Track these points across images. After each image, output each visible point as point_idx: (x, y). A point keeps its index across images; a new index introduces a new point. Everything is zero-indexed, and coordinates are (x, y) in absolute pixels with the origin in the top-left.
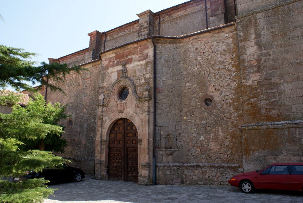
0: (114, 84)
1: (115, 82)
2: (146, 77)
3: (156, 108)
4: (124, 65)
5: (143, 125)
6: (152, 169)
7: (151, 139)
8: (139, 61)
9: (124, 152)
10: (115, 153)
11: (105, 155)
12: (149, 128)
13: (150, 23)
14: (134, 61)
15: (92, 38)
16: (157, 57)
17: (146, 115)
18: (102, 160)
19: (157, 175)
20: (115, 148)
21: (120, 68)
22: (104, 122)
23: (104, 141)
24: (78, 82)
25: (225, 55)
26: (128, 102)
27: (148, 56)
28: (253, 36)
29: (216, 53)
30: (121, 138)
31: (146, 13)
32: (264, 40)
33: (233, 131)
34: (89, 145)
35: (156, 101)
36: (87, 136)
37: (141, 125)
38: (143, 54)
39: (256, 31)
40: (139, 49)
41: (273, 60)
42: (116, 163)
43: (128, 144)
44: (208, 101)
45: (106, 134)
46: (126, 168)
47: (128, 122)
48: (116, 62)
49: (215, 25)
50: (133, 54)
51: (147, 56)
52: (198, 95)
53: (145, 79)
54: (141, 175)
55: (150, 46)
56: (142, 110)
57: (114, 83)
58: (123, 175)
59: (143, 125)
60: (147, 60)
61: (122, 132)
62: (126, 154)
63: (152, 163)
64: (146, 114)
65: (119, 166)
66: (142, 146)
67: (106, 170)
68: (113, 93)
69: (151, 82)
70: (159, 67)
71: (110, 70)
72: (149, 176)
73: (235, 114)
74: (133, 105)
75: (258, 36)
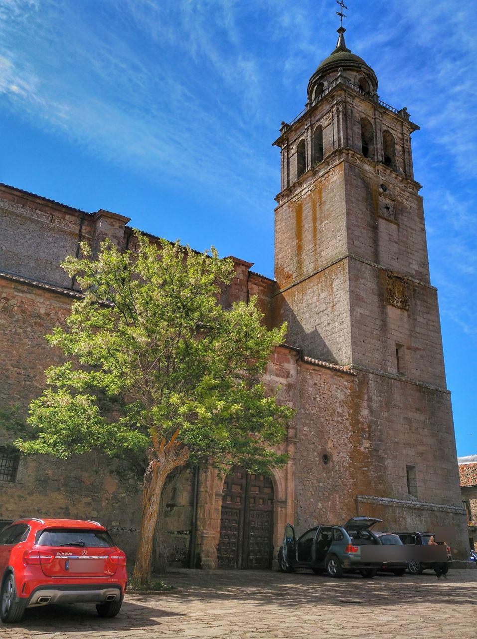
25: (344, 407)
28: (366, 397)
29: (336, 400)
31: (119, 220)
33: (349, 502)
41: (380, 431)
44: (326, 458)
52: (316, 447)
55: (292, 361)
65: (234, 543)
73: (351, 482)
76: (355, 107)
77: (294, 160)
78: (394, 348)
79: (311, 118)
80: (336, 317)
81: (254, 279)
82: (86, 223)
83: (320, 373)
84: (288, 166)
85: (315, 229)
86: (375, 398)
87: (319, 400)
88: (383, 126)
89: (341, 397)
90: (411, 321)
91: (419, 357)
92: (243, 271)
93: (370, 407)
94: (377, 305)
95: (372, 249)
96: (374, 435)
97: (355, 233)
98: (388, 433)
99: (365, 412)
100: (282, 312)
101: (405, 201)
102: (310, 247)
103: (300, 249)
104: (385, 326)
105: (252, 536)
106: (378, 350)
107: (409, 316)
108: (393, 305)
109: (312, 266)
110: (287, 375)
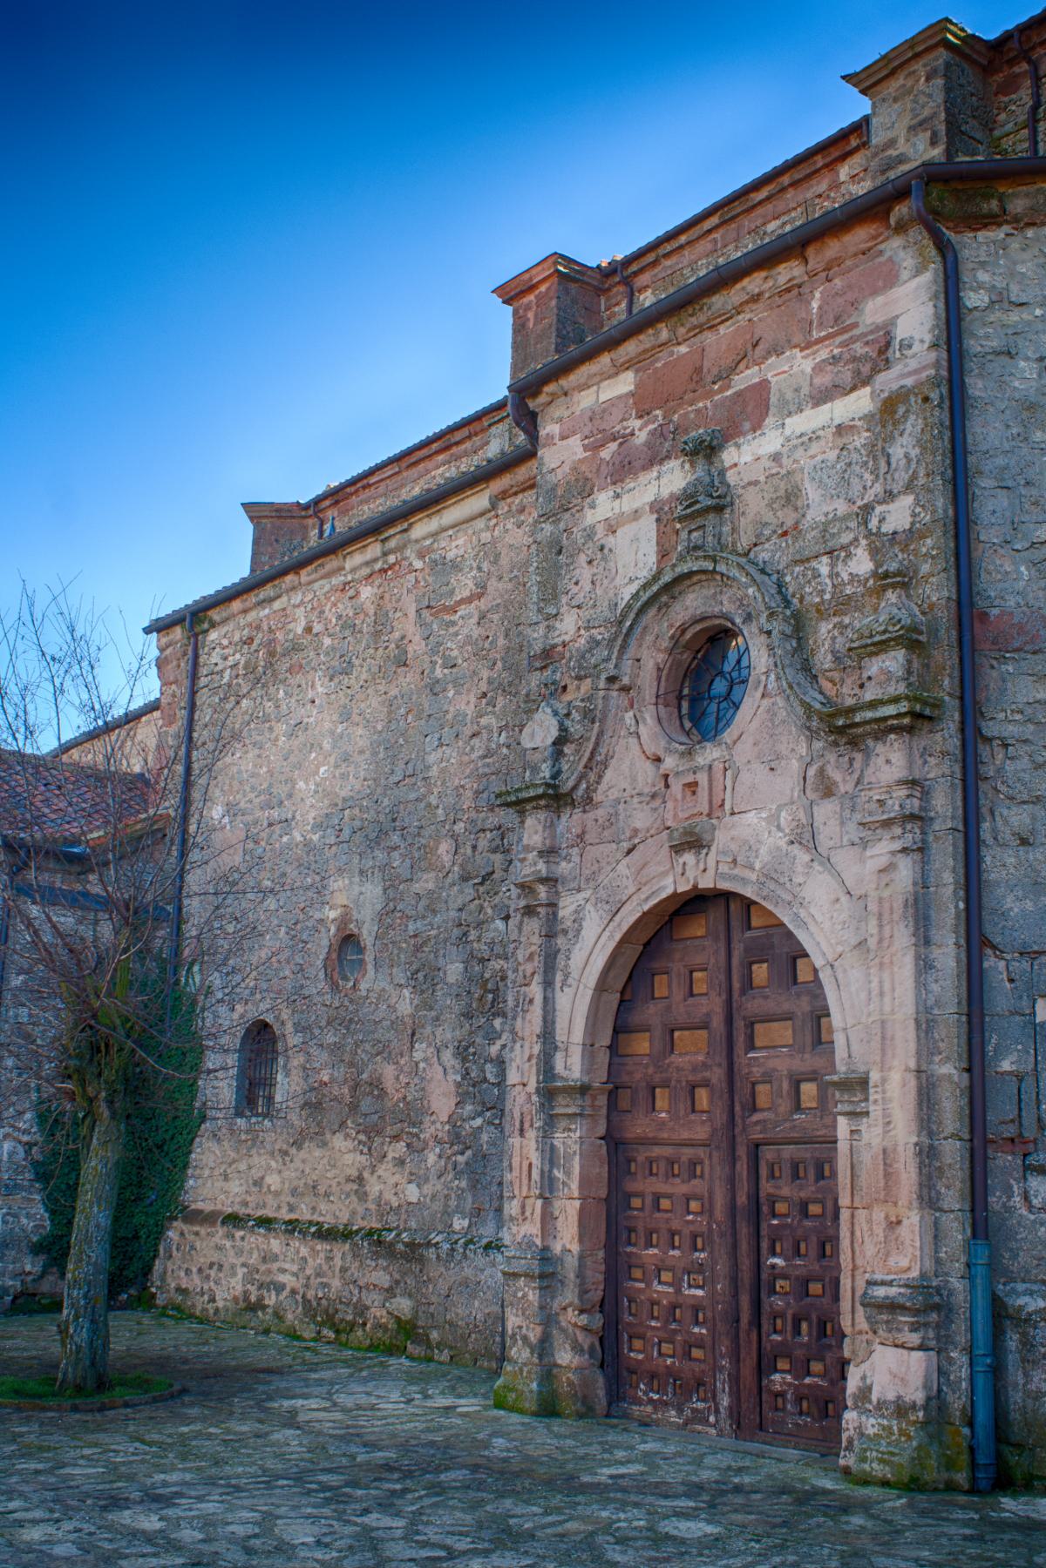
0: (632, 615)
1: (636, 596)
2: (887, 528)
3: (983, 786)
4: (706, 450)
5: (872, 943)
6: (962, 1339)
7: (948, 1070)
8: (821, 397)
9: (732, 1181)
10: (662, 1187)
11: (577, 1203)
12: (924, 966)
13: (951, 123)
14: (783, 402)
15: (531, 315)
16: (973, 345)
17: (893, 853)
18: (557, 1248)
19: (1016, 1398)
20: (657, 1151)
21: (674, 478)
22: (565, 932)
23: (569, 1091)
24: (397, 635)
26: (744, 751)
27: (888, 344)
30: (705, 1066)
34: (479, 1122)
35: (979, 731)
36: (462, 1052)
37: (854, 942)
38: (853, 340)
40: (815, 305)
42: (666, 1276)
43: (756, 1117)
45: (578, 1035)
46: (745, 1318)
47: (755, 922)
48: (642, 437)
50: (769, 354)
51: (884, 348)
53: (880, 544)
54: (865, 1392)
55: (907, 261)
56: (858, 817)
57: (629, 606)
58: (722, 1384)
59: (872, 943)
60: (889, 380)
61: (708, 1015)
62: (742, 1199)
63: (957, 1284)
64: (897, 845)
66: (872, 1134)
67: (585, 1329)
68: (625, 689)
69: (925, 568)
70: (987, 431)
71: (604, 505)
72: (936, 1403)
74: (787, 783)
105: (776, 1273)
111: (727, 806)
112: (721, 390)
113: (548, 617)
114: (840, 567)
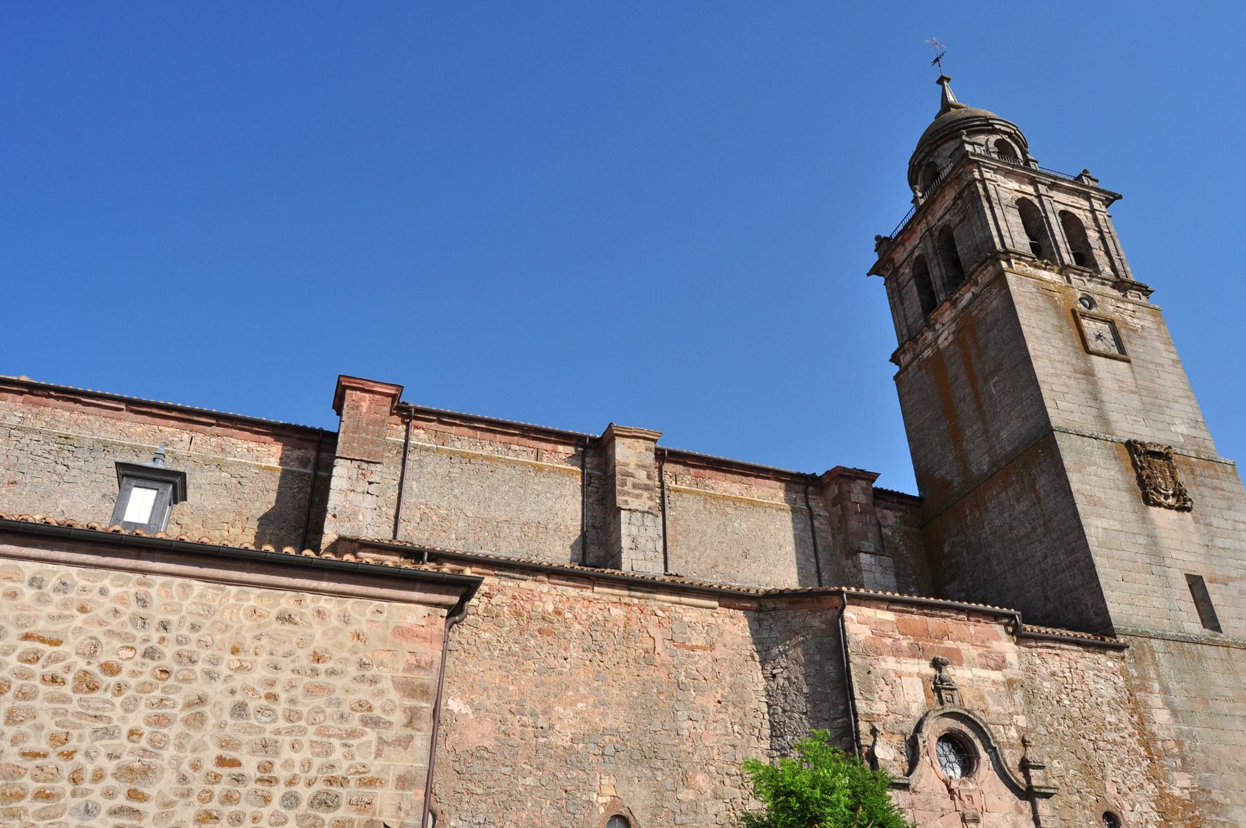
14: (969, 662)
28: (1156, 686)
32: (1179, 700)
39: (1159, 676)
41: (1203, 751)
48: (905, 643)
49: (875, 578)
75: (1165, 690)
76: (1001, 184)
77: (913, 292)
78: (1184, 584)
79: (926, 219)
80: (1057, 543)
81: (884, 500)
82: (591, 452)
83: (1058, 652)
84: (902, 304)
85: (977, 395)
86: (1173, 685)
87: (1068, 703)
88: (1056, 204)
89: (1108, 692)
90: (1203, 529)
91: (1236, 593)
92: (863, 489)
93: (1169, 705)
94: (1129, 507)
95: (1095, 412)
96: (1193, 760)
97: (1055, 387)
98: (1219, 753)
99: (1161, 716)
100: (946, 549)
101: (1129, 319)
102: (975, 428)
103: (956, 435)
104: (1156, 544)
106: (1154, 591)
107: (1196, 521)
108: (1160, 505)
109: (986, 459)
110: (1001, 665)
111: (985, 809)
112: (938, 643)
113: (867, 699)
114: (1007, 732)
